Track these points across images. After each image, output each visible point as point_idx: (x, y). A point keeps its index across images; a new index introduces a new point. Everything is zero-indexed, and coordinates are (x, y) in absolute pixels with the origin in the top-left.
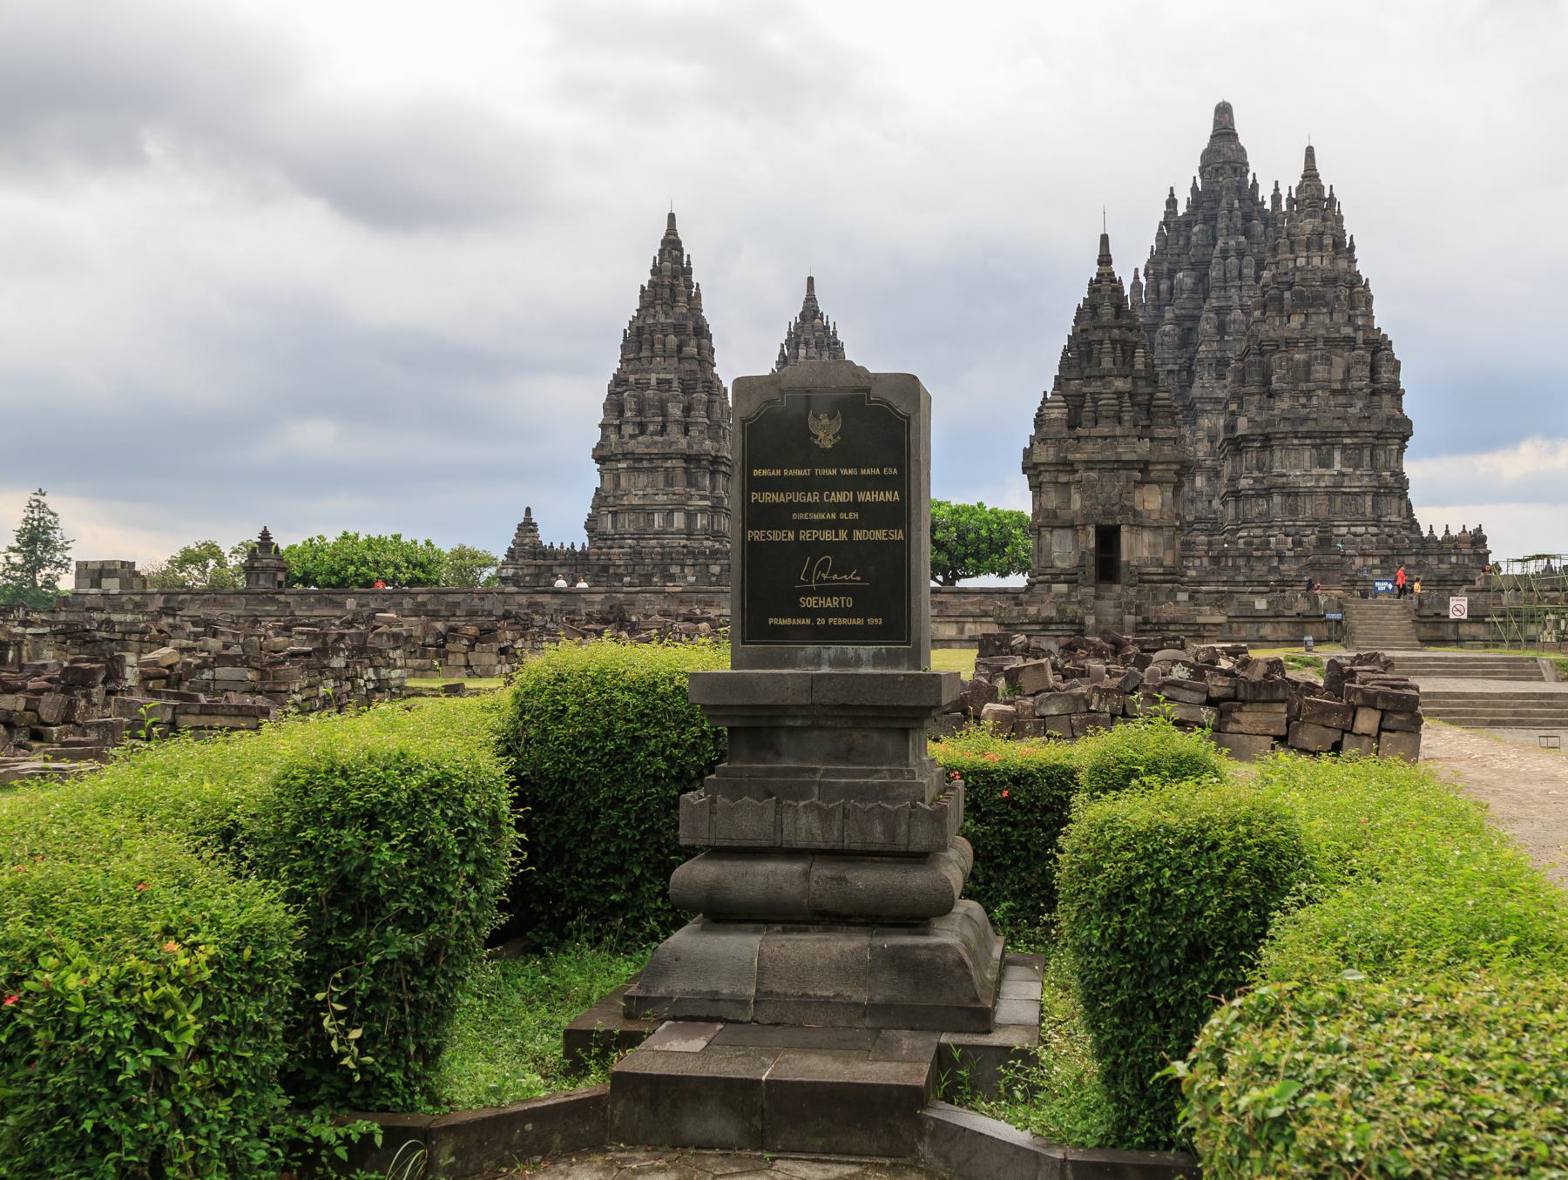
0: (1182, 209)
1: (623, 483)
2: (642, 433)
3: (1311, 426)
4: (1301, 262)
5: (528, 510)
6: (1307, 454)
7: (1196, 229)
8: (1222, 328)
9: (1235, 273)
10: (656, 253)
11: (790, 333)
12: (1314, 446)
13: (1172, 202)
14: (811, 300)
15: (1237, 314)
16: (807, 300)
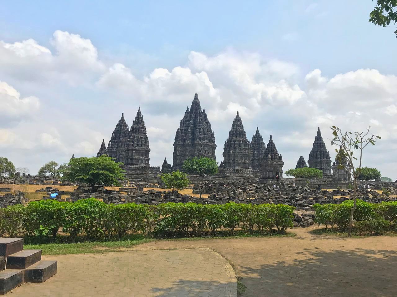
0: (189, 110)
1: (134, 154)
2: (138, 146)
3: (241, 153)
4: (238, 129)
5: (73, 155)
6: (240, 158)
7: (193, 114)
8: (200, 132)
9: (201, 123)
10: (137, 114)
11: (118, 123)
12: (241, 156)
13: (188, 109)
14: (123, 117)
15: (202, 130)
16: (122, 118)
